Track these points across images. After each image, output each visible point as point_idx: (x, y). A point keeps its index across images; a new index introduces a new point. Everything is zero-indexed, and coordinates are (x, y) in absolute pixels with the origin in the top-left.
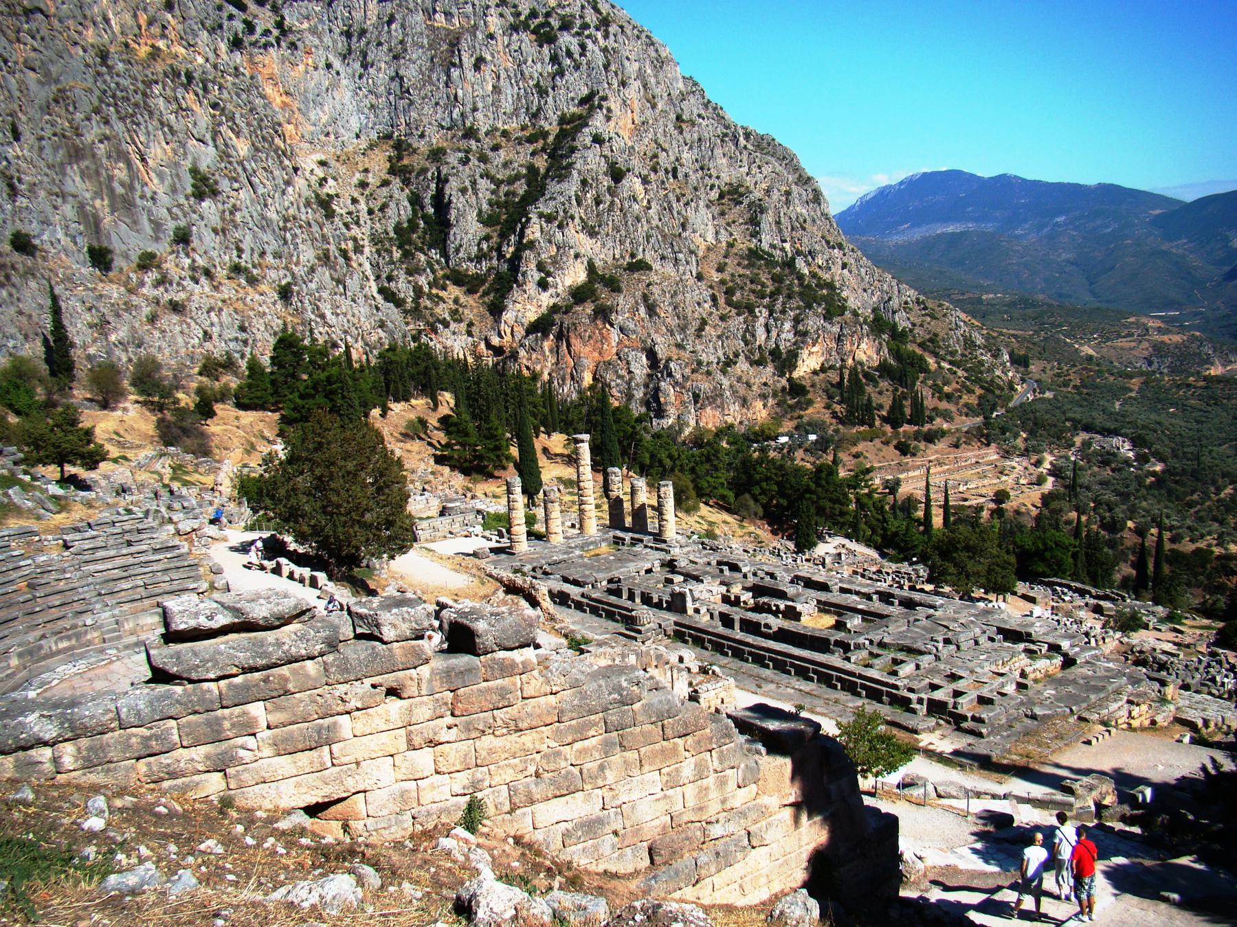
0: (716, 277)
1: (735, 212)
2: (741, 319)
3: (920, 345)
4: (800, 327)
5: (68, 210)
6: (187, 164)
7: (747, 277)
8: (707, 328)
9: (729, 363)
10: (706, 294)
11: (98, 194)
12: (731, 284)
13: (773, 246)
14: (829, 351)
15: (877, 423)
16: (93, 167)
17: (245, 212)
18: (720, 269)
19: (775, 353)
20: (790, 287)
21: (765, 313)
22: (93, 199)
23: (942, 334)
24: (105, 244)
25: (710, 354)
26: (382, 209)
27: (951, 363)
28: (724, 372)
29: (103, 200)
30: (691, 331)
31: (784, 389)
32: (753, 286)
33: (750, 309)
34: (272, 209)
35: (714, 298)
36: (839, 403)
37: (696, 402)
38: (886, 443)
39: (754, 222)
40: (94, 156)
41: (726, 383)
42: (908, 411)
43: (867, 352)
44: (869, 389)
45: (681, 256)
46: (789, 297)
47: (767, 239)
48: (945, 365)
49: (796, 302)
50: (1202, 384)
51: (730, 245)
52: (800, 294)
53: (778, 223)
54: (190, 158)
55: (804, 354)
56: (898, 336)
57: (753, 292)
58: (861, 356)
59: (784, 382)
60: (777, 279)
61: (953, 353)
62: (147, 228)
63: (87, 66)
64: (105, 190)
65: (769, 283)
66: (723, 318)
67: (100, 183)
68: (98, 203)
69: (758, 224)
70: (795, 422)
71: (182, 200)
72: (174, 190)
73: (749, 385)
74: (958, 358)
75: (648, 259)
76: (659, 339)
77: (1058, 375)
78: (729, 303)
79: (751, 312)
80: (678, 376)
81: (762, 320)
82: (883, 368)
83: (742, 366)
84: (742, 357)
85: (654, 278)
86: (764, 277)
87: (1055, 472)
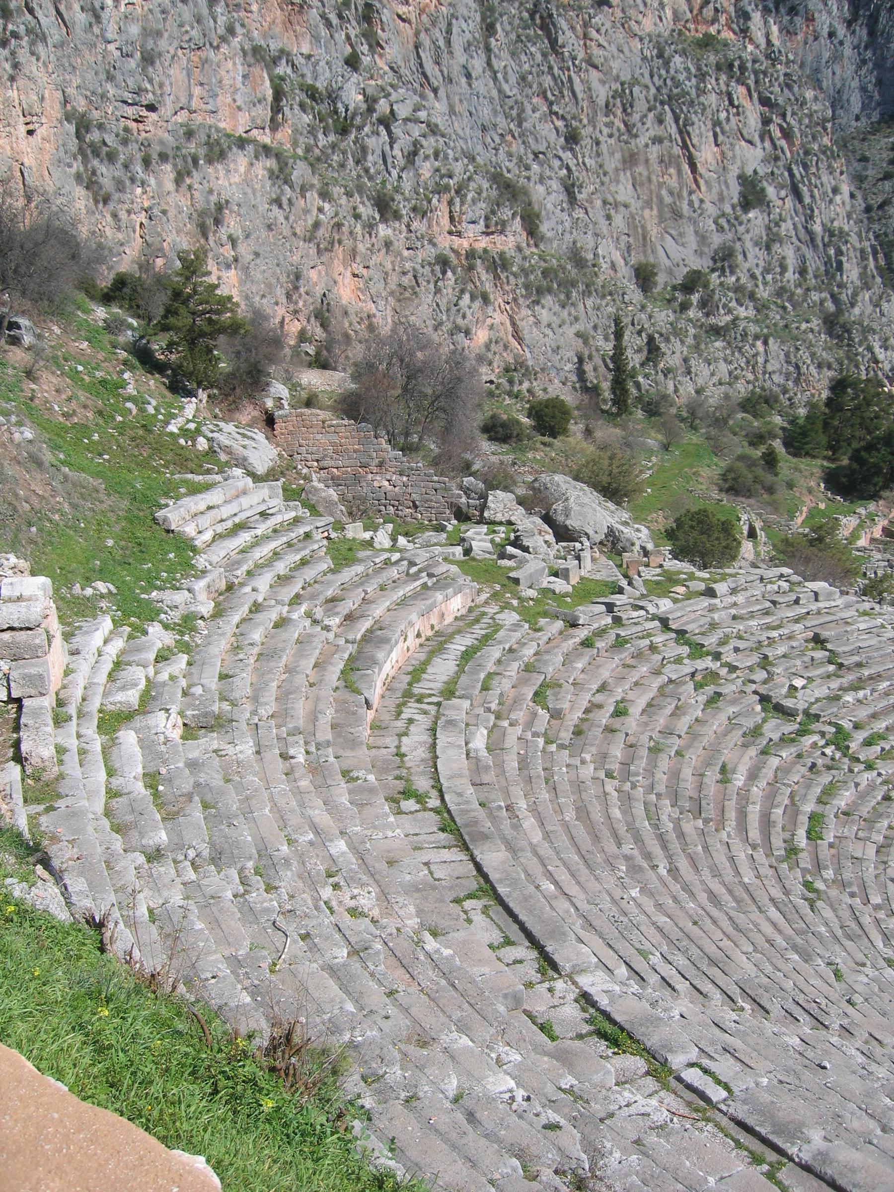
5: (619, 220)
6: (734, 171)
11: (648, 204)
16: (645, 173)
17: (789, 223)
22: (642, 208)
24: (652, 260)
26: (881, 207)
29: (651, 209)
34: (818, 221)
40: (647, 161)
54: (739, 163)
62: (691, 240)
63: (645, 58)
64: (655, 199)
67: (651, 191)
68: (647, 212)
71: (728, 209)
72: (721, 199)
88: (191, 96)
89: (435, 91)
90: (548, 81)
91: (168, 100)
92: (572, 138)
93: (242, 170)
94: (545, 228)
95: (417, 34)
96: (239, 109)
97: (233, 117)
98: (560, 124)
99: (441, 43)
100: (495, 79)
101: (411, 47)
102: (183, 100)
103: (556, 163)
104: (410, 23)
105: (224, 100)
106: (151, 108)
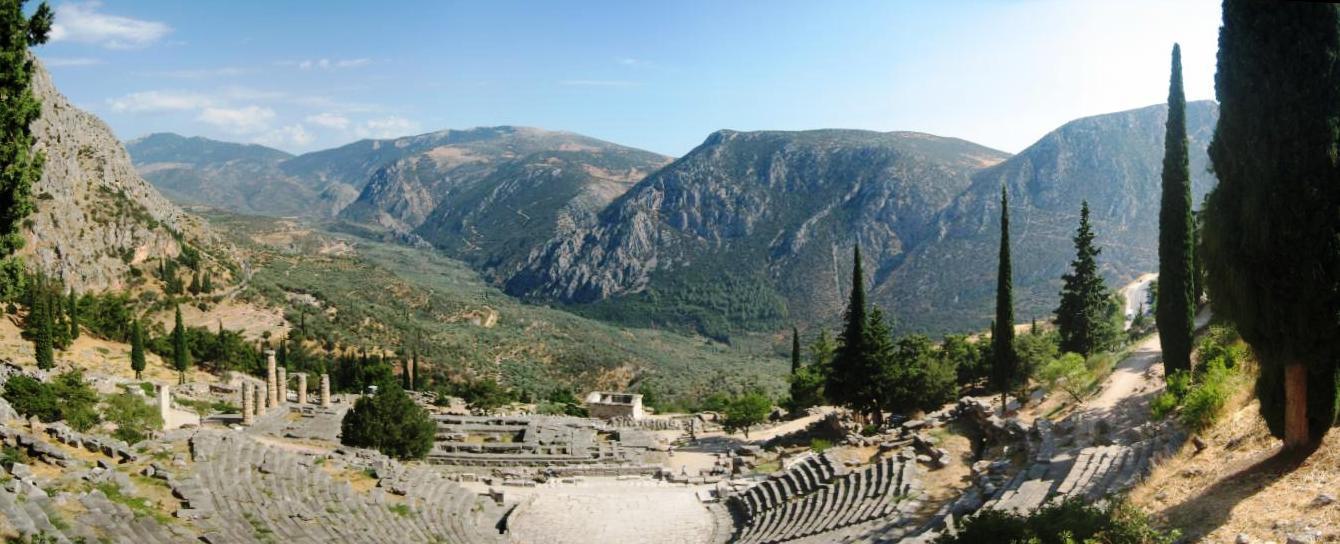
0: (84, 203)
1: (89, 163)
2: (101, 229)
3: (190, 242)
4: (135, 234)
7: (102, 203)
8: (85, 235)
9: (97, 257)
10: (81, 213)
12: (93, 208)
13: (111, 184)
14: (151, 249)
15: (185, 292)
18: (86, 198)
19: (121, 250)
20: (126, 210)
21: (115, 225)
23: (200, 236)
25: (88, 251)
27: (209, 253)
28: (96, 261)
30: (76, 237)
31: (128, 272)
32: (106, 209)
33: (106, 222)
35: (85, 216)
36: (162, 280)
37: (84, 280)
38: (194, 305)
39: (100, 169)
41: (100, 269)
42: (201, 285)
43: (173, 250)
44: (176, 271)
45: (67, 190)
46: (128, 216)
47: (108, 179)
48: (205, 254)
49: (131, 219)
50: (329, 260)
51: (90, 184)
52: (134, 215)
53: (113, 170)
55: (137, 250)
56: (178, 237)
57: (106, 212)
58: (169, 251)
59: (128, 269)
60: (118, 205)
61: (207, 247)
65: (115, 207)
66: (91, 228)
69: (103, 171)
70: (139, 292)
73: (109, 270)
74: (210, 250)
75: (50, 192)
76: (61, 242)
77: (252, 257)
78: (94, 219)
79: (107, 225)
80: (73, 265)
81: (112, 231)
82: (180, 258)
83: (105, 258)
84: (104, 253)
85: (56, 204)
86: (111, 203)
87: (288, 318)
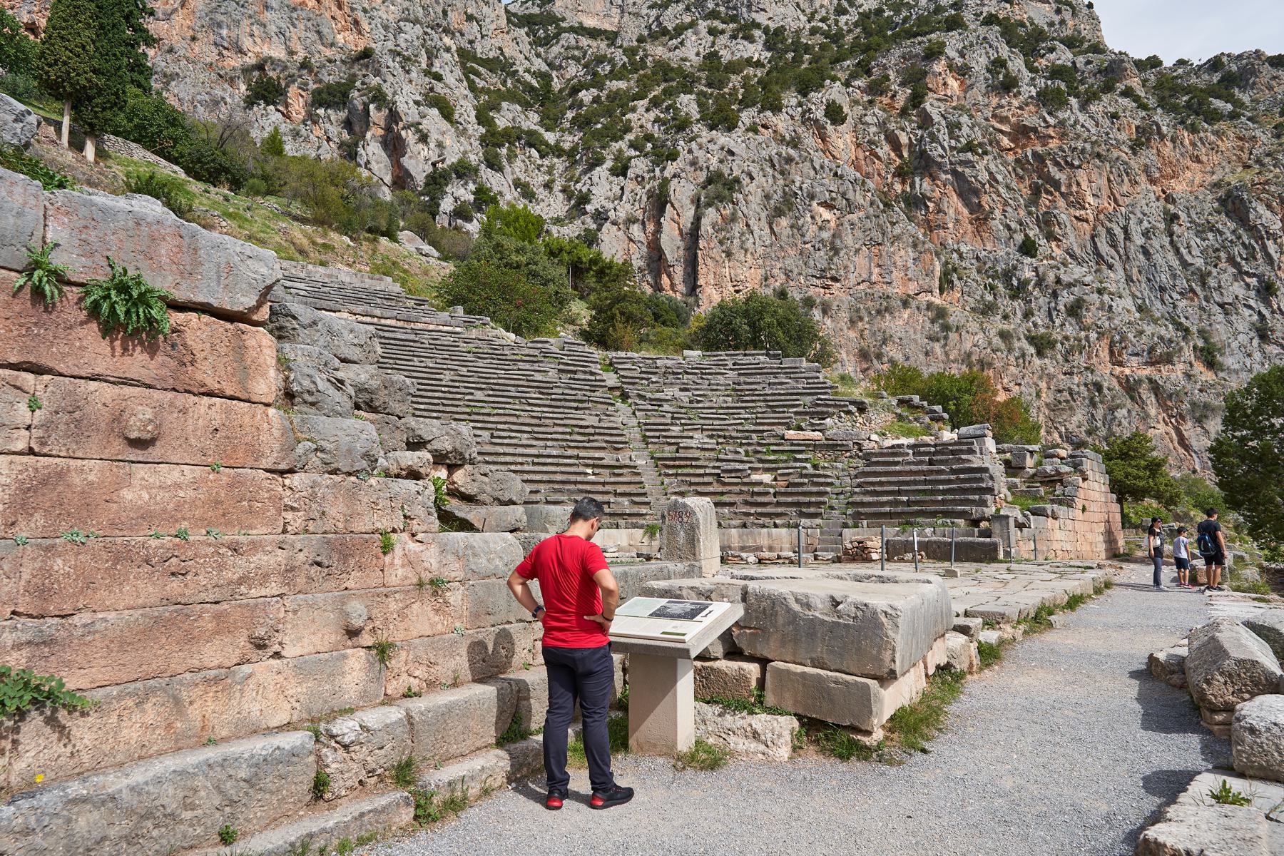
88: (871, 274)
89: (1110, 267)
90: (1237, 250)
91: (852, 276)
92: (1266, 290)
93: (906, 316)
94: (1229, 361)
95: (1094, 228)
96: (910, 280)
97: (904, 285)
98: (1253, 281)
99: (1118, 231)
100: (1177, 251)
101: (1088, 237)
102: (865, 276)
103: (1247, 312)
104: (1087, 221)
105: (897, 275)
106: (835, 279)
